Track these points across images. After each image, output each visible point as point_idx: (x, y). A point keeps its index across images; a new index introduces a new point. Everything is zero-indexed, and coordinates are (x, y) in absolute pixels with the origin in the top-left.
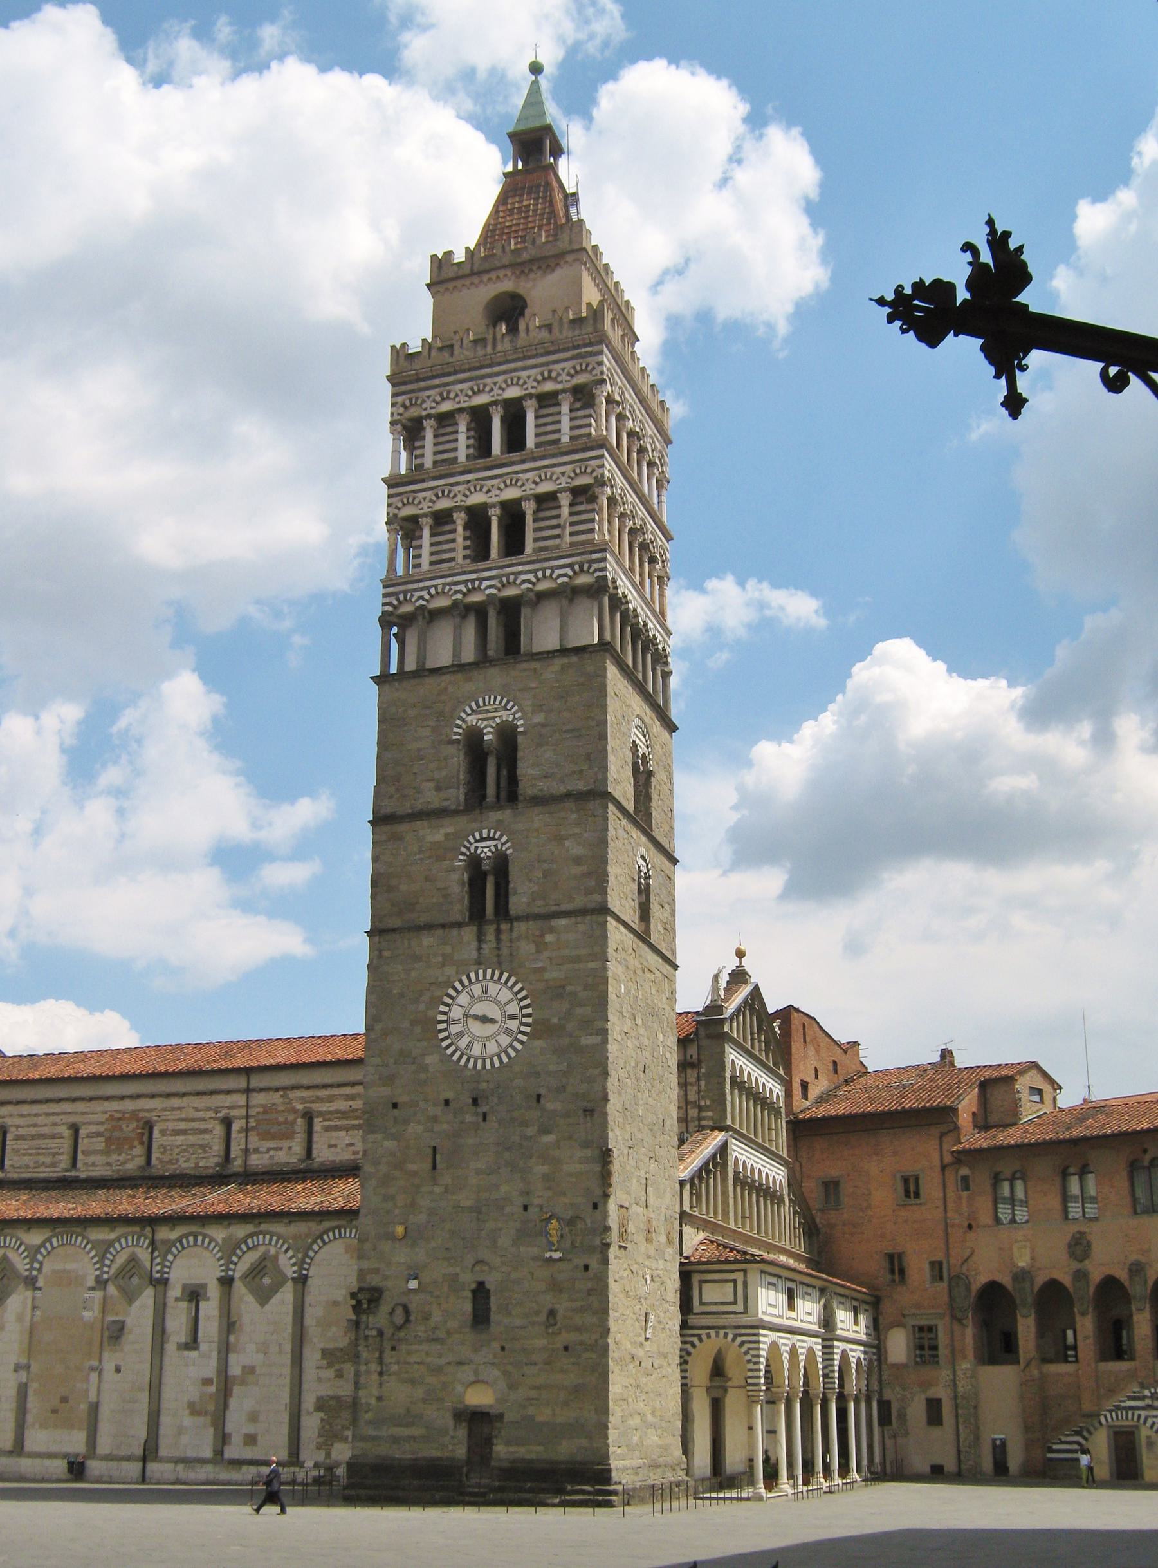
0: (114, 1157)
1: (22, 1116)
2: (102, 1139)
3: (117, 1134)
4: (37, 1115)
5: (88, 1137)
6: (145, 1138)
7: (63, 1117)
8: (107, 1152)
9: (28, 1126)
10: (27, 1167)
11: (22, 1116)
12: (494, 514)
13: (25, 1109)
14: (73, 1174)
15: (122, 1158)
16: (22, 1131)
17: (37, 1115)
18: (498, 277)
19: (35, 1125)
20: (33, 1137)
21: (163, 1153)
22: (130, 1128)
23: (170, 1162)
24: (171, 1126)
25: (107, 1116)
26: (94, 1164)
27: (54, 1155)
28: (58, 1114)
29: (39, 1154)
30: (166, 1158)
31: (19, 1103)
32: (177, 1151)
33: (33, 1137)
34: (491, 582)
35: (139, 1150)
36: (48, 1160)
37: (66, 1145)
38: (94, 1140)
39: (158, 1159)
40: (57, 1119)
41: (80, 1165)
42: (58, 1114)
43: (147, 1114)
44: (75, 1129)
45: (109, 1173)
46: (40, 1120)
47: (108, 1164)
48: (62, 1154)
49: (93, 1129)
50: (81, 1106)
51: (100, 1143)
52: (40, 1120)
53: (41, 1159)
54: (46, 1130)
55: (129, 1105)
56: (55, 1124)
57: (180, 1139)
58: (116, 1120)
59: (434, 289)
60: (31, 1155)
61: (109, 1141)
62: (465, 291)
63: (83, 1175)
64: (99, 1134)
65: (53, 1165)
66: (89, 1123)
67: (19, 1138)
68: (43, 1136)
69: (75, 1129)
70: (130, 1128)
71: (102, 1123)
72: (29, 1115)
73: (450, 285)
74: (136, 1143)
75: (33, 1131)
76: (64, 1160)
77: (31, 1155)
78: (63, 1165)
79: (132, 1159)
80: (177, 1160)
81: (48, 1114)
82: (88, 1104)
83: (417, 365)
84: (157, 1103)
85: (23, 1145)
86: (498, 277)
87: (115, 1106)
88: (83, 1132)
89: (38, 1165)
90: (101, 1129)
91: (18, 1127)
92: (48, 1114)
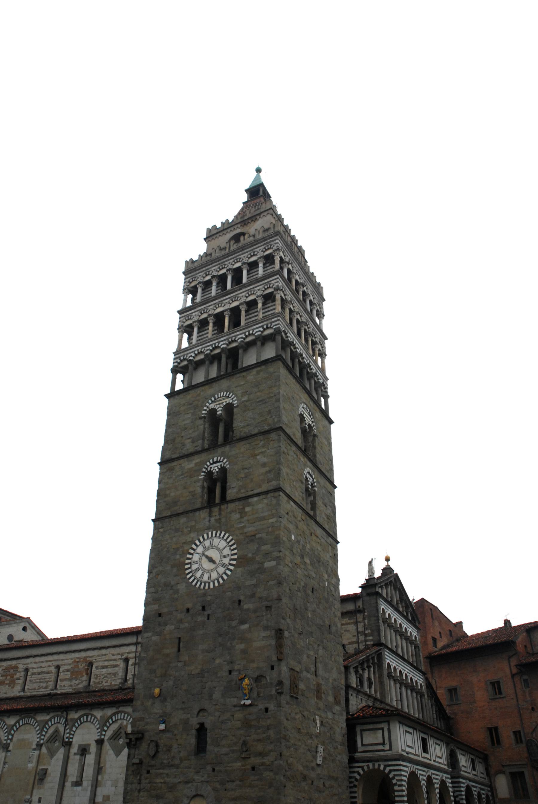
0: (74, 682)
1: (36, 663)
2: (69, 673)
3: (76, 669)
4: (42, 662)
5: (63, 672)
6: (89, 672)
7: (53, 662)
8: (70, 680)
9: (38, 668)
10: (35, 689)
11: (36, 663)
13: (37, 659)
14: (55, 691)
15: (77, 682)
16: (35, 671)
17: (42, 662)
18: (234, 229)
19: (41, 667)
20: (39, 673)
21: (96, 678)
22: (82, 666)
23: (99, 683)
24: (101, 664)
25: (73, 660)
26: (64, 686)
27: (47, 682)
28: (51, 661)
29: (40, 682)
30: (97, 681)
31: (35, 656)
32: (102, 677)
33: (39, 673)
35: (85, 678)
36: (44, 685)
37: (53, 676)
38: (66, 673)
39: (93, 681)
40: (50, 663)
41: (58, 687)
42: (51, 661)
43: (90, 659)
44: (58, 667)
45: (71, 690)
46: (43, 665)
47: (71, 686)
48: (51, 681)
49: (66, 667)
50: (62, 656)
51: (68, 675)
52: (43, 665)
53: (42, 684)
54: (45, 670)
55: (83, 654)
56: (49, 666)
57: (104, 671)
58: (76, 662)
59: (207, 240)
60: (37, 682)
61: (72, 674)
62: (220, 238)
63: (59, 692)
64: (68, 670)
65: (46, 687)
66: (64, 665)
67: (33, 674)
68: (43, 673)
69: (58, 667)
70: (82, 666)
71: (70, 664)
72: (39, 662)
73: (214, 237)
74: (84, 674)
75: (40, 670)
76: (51, 684)
77: (37, 682)
78: (50, 687)
79: (82, 682)
80: (102, 682)
81: (47, 661)
82: (65, 655)
83: (196, 264)
84: (95, 653)
85: (34, 677)
86: (234, 229)
87: (77, 655)
88: (61, 670)
89: (40, 688)
90: (69, 667)
91: (33, 668)
92: (47, 661)
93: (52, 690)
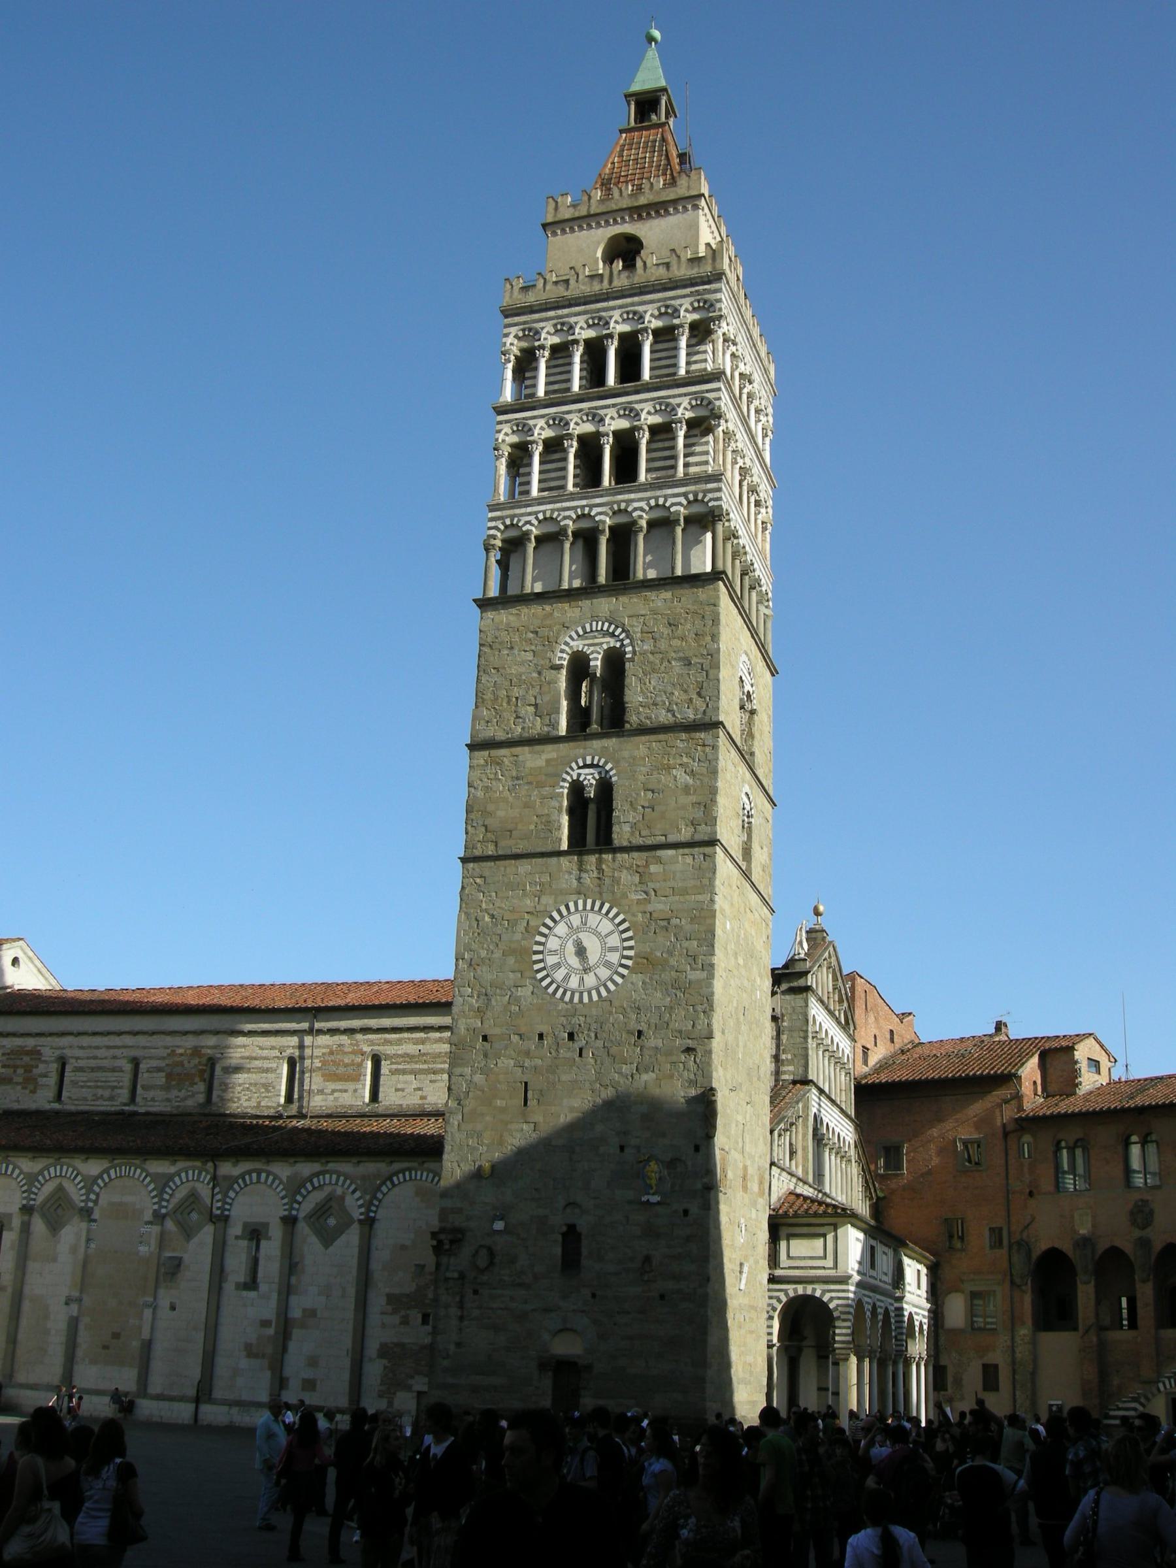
0: (175, 1093)
2: (163, 1074)
3: (178, 1070)
5: (148, 1071)
6: (206, 1076)
8: (167, 1088)
15: (182, 1094)
25: (169, 1051)
26: (153, 1100)
35: (201, 1087)
38: (155, 1074)
45: (169, 1109)
47: (168, 1100)
49: (154, 1063)
50: (142, 1040)
51: (160, 1079)
61: (169, 1076)
64: (159, 1070)
66: (150, 1058)
70: (192, 1065)
71: (164, 1058)
74: (197, 1079)
79: (193, 1096)
82: (150, 1038)
88: (143, 1066)
90: (162, 1064)
93: (125, 1105)
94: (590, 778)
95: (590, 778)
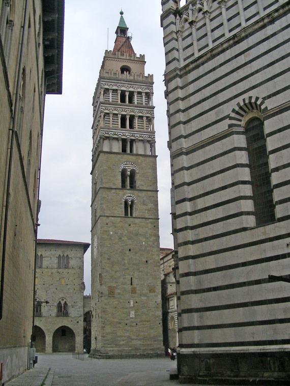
12: (128, 117)
34: (127, 134)
94: (130, 200)
95: (130, 200)
